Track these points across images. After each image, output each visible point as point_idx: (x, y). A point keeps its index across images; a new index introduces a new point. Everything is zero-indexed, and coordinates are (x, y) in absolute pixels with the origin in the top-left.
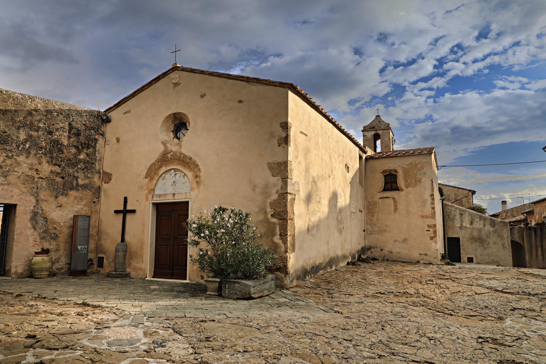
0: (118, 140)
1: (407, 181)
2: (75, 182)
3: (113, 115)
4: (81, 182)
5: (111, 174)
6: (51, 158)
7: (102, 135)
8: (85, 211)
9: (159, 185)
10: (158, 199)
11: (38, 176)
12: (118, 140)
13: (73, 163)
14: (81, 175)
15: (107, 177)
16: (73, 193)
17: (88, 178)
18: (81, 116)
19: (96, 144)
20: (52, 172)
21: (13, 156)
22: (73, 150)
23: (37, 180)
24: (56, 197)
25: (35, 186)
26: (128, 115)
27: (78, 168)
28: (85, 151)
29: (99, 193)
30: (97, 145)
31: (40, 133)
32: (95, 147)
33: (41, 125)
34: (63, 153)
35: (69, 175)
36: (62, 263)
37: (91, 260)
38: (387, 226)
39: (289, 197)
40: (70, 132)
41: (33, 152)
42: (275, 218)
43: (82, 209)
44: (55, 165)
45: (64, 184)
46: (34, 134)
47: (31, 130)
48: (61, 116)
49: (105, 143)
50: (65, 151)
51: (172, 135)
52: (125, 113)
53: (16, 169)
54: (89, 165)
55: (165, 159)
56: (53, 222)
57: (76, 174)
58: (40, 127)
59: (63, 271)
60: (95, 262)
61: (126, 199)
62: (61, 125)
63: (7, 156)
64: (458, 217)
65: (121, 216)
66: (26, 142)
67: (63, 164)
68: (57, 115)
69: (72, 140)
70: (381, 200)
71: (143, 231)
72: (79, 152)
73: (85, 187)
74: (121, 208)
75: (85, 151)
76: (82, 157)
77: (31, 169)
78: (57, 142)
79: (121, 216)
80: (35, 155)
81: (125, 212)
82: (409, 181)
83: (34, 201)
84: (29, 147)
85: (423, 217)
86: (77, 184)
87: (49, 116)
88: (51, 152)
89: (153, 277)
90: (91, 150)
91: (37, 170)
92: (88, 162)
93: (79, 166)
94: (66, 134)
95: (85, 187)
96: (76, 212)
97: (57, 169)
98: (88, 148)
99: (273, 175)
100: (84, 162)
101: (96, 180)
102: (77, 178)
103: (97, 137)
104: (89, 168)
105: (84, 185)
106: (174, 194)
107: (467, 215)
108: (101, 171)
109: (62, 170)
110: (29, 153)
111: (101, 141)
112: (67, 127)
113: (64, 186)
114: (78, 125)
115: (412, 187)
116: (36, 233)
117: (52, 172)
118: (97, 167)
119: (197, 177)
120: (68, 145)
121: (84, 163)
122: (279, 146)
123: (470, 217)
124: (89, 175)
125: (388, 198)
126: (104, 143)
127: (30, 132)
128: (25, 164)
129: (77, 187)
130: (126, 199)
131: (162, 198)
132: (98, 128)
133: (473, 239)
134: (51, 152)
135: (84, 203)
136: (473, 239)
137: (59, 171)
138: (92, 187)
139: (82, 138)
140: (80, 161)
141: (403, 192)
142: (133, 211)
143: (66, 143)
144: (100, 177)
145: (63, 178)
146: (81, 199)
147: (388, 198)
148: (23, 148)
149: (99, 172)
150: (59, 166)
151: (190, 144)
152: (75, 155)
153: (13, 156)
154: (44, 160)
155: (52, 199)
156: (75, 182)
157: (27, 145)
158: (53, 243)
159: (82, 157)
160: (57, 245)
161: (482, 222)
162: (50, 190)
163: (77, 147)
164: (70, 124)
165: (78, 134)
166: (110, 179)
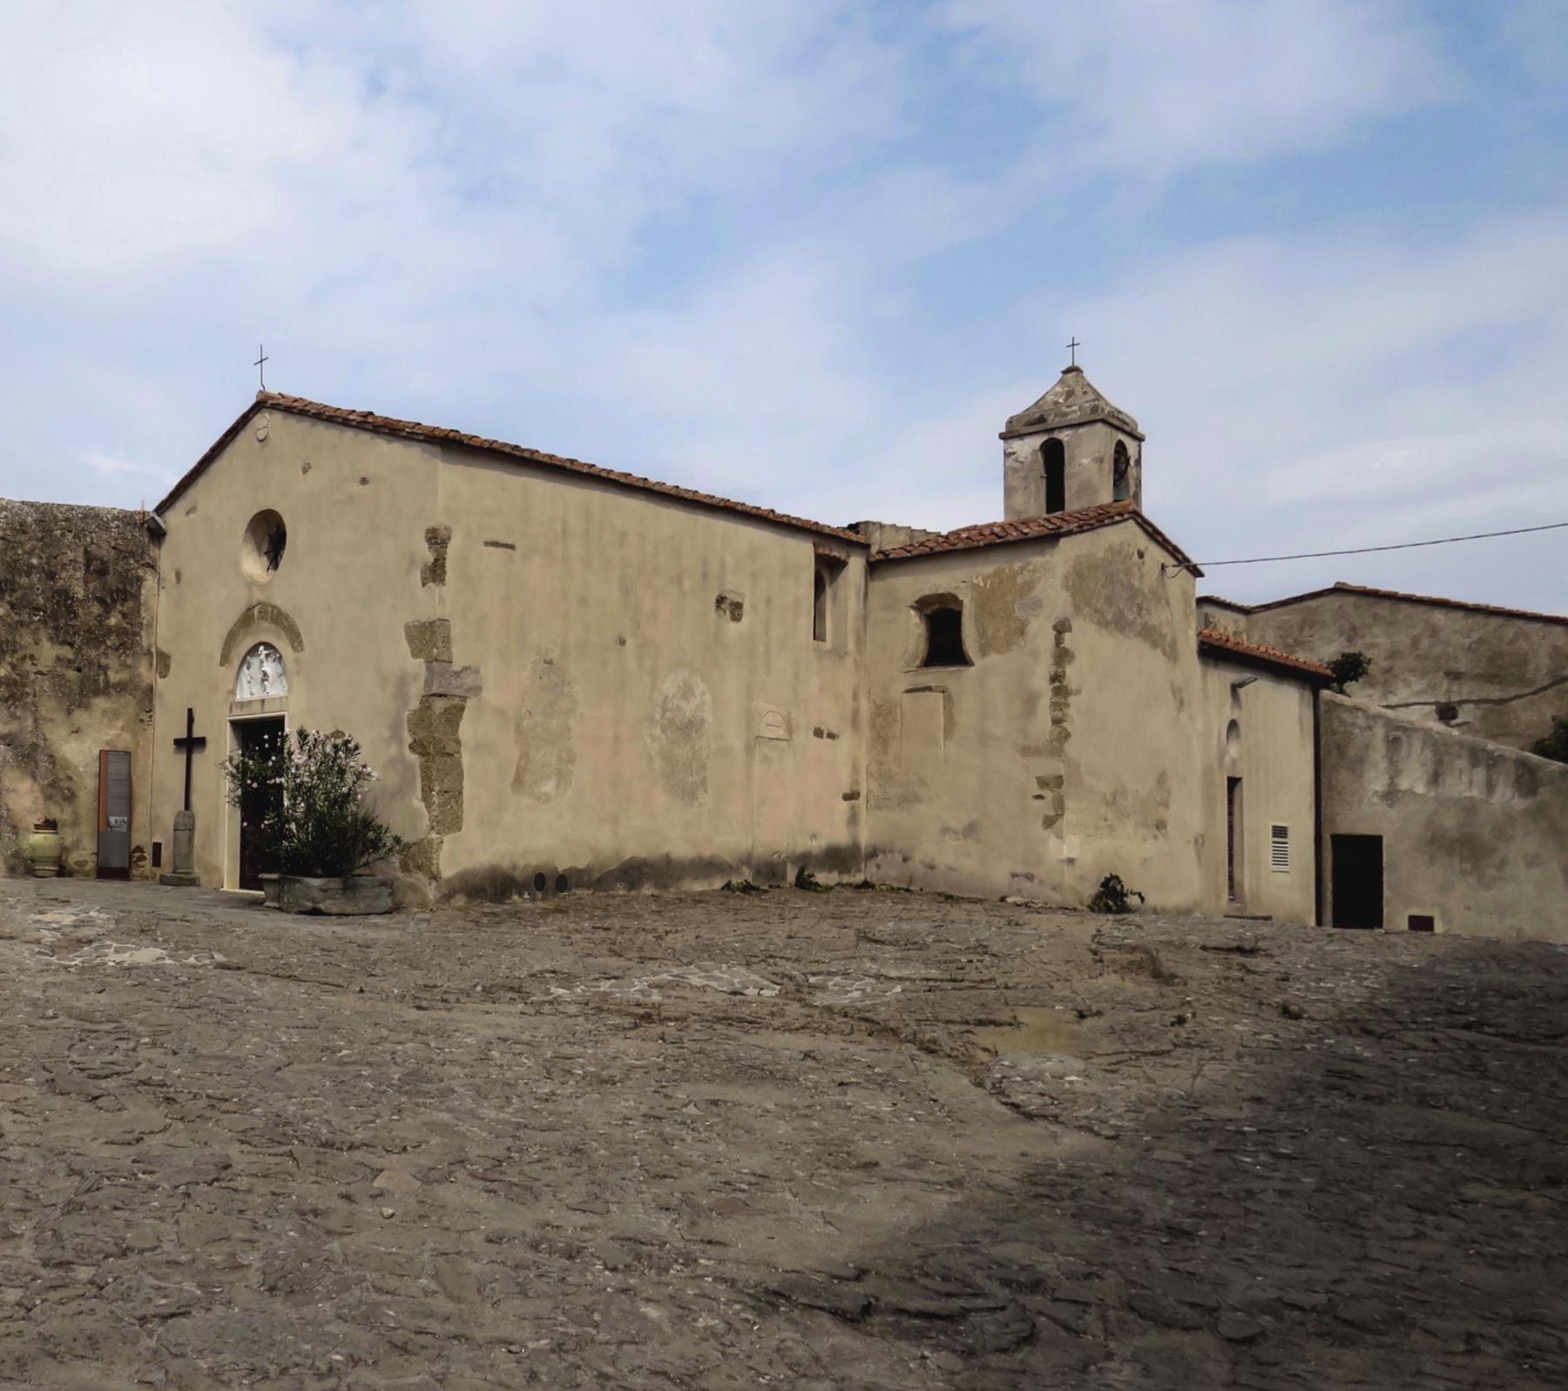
0: (178, 576)
2: (101, 678)
3: (173, 520)
4: (114, 677)
6: (56, 628)
7: (152, 567)
8: (125, 741)
11: (35, 669)
12: (178, 576)
13: (96, 636)
14: (112, 661)
15: (163, 663)
16: (100, 703)
18: (108, 529)
20: (58, 658)
22: (96, 609)
24: (69, 712)
27: (108, 647)
28: (119, 607)
29: (151, 701)
31: (35, 578)
32: (137, 597)
33: (35, 561)
34: (76, 615)
35: (91, 663)
36: (85, 854)
37: (139, 849)
38: (923, 783)
40: (87, 570)
43: (118, 736)
44: (64, 643)
45: (82, 685)
48: (70, 536)
50: (81, 611)
54: (128, 640)
56: (66, 765)
57: (103, 661)
58: (31, 566)
59: (87, 868)
60: (148, 854)
61: (190, 711)
62: (71, 555)
64: (1379, 752)
67: (78, 640)
69: (91, 585)
70: (907, 698)
72: (108, 610)
73: (122, 687)
76: (113, 621)
78: (63, 597)
85: (1026, 751)
86: (107, 682)
87: (47, 540)
88: (54, 616)
90: (130, 604)
94: (79, 575)
95: (122, 687)
96: (107, 743)
97: (67, 653)
98: (125, 600)
100: (120, 632)
101: (146, 673)
102: (104, 669)
103: (140, 572)
107: (1417, 746)
111: (150, 582)
113: (84, 689)
114: (104, 551)
115: (1000, 652)
116: (36, 787)
117: (58, 658)
118: (145, 642)
120: (86, 599)
121: (118, 635)
123: (1428, 754)
125: (929, 689)
129: (105, 690)
133: (1437, 843)
134: (54, 616)
135: (120, 724)
136: (1437, 843)
137: (71, 656)
138: (137, 688)
139: (111, 579)
140: (110, 630)
141: (972, 670)
143: (80, 592)
145: (79, 670)
146: (116, 714)
147: (929, 689)
149: (149, 653)
150: (71, 645)
152: (100, 620)
154: (43, 636)
155: (60, 717)
156: (101, 678)
158: (68, 809)
159: (113, 621)
160: (75, 813)
161: (1480, 775)
162: (56, 696)
163: (101, 601)
164: (86, 552)
165: (102, 572)
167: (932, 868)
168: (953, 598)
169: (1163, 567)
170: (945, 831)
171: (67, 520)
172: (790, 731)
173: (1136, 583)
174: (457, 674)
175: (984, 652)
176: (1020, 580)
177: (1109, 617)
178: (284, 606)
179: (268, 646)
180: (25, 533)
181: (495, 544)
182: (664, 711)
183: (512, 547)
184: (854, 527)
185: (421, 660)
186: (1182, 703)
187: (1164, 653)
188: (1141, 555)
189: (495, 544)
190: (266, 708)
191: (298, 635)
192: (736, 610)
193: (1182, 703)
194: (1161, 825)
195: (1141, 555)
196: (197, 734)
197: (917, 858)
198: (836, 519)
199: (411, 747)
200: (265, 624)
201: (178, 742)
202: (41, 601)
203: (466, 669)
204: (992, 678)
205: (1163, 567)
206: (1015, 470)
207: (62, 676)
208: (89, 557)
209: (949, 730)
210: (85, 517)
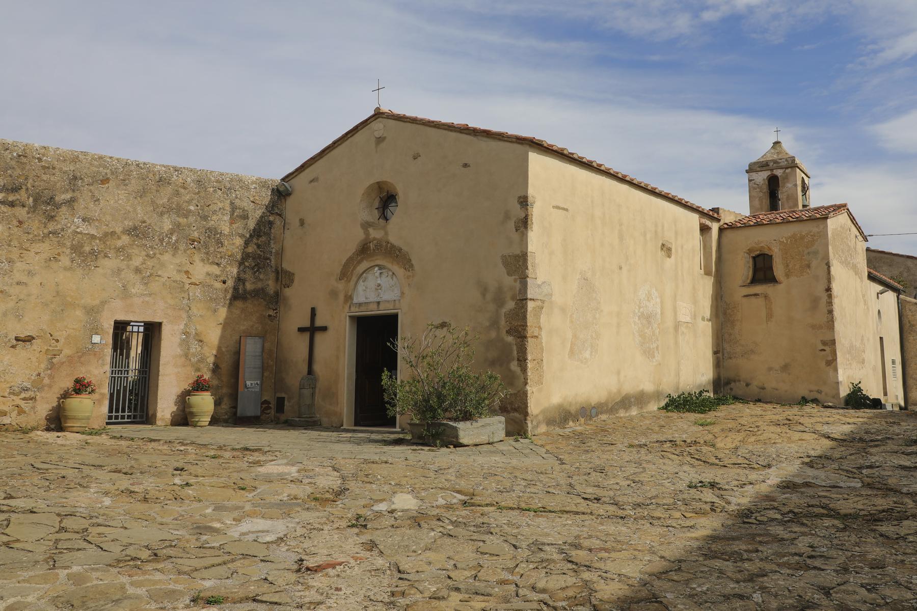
0: (302, 223)
5: (293, 274)
6: (207, 253)
7: (280, 215)
9: (361, 287)
10: (357, 310)
12: (302, 223)
17: (261, 280)
18: (248, 189)
19: (270, 228)
21: (155, 254)
23: (187, 286)
25: (186, 296)
26: (316, 183)
27: (246, 267)
30: (273, 231)
31: (191, 219)
32: (269, 234)
33: (192, 208)
39: (530, 305)
40: (232, 214)
41: (182, 247)
42: (511, 335)
44: (213, 263)
46: (183, 221)
47: (178, 216)
48: (219, 192)
50: (226, 243)
51: (376, 213)
52: (311, 181)
53: (160, 273)
58: (190, 211)
61: (313, 310)
62: (220, 205)
63: (148, 256)
65: (307, 336)
66: (172, 234)
67: (224, 262)
68: (215, 191)
71: (338, 354)
74: (307, 324)
75: (255, 240)
77: (179, 271)
78: (213, 233)
79: (307, 336)
80: (185, 251)
81: (312, 330)
83: (184, 315)
84: (177, 241)
86: (245, 290)
87: (202, 194)
89: (355, 425)
90: (263, 239)
91: (187, 272)
92: (260, 256)
93: (247, 264)
94: (227, 218)
97: (216, 270)
104: (261, 266)
105: (254, 291)
106: (378, 303)
109: (222, 271)
110: (176, 249)
112: (228, 208)
117: (208, 274)
121: (254, 259)
124: (261, 276)
127: (177, 219)
128: (170, 265)
130: (313, 310)
131: (363, 308)
137: (218, 273)
142: (324, 329)
143: (226, 230)
145: (224, 282)
148: (169, 243)
153: (155, 254)
154: (197, 258)
157: (174, 238)
164: (232, 203)
166: (292, 281)
167: (763, 388)
170: (770, 369)
171: (218, 181)
174: (539, 286)
175: (787, 276)
179: (381, 267)
180: (185, 188)
181: (558, 207)
182: (640, 308)
183: (567, 210)
184: (713, 210)
189: (558, 207)
190: (382, 307)
194: (863, 362)
196: (319, 323)
197: (755, 383)
201: (301, 330)
202: (196, 234)
203: (544, 283)
204: (786, 292)
206: (755, 189)
207: (210, 286)
208: (234, 207)
209: (770, 316)
210: (231, 180)
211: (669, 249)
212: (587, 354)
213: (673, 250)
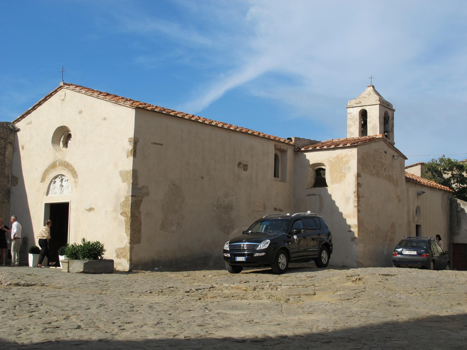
1: (333, 176)
5: (18, 178)
7: (11, 143)
19: (5, 152)
26: (30, 125)
30: (7, 153)
49: (13, 150)
52: (28, 124)
55: (53, 166)
82: (334, 177)
99: (123, 182)
108: (10, 175)
119: (75, 182)
122: (128, 157)
126: (12, 151)
132: (7, 138)
144: (9, 181)
149: (8, 176)
151: (72, 153)
168: (323, 165)
169: (393, 156)
172: (265, 208)
173: (384, 162)
176: (344, 160)
177: (374, 172)
178: (71, 162)
185: (125, 184)
186: (400, 200)
187: (394, 184)
188: (386, 152)
191: (75, 172)
192: (245, 167)
193: (400, 200)
195: (386, 152)
198: (283, 137)
199: (121, 214)
200: (60, 167)
205: (393, 156)
211: (246, 166)
212: (174, 228)
213: (249, 166)
